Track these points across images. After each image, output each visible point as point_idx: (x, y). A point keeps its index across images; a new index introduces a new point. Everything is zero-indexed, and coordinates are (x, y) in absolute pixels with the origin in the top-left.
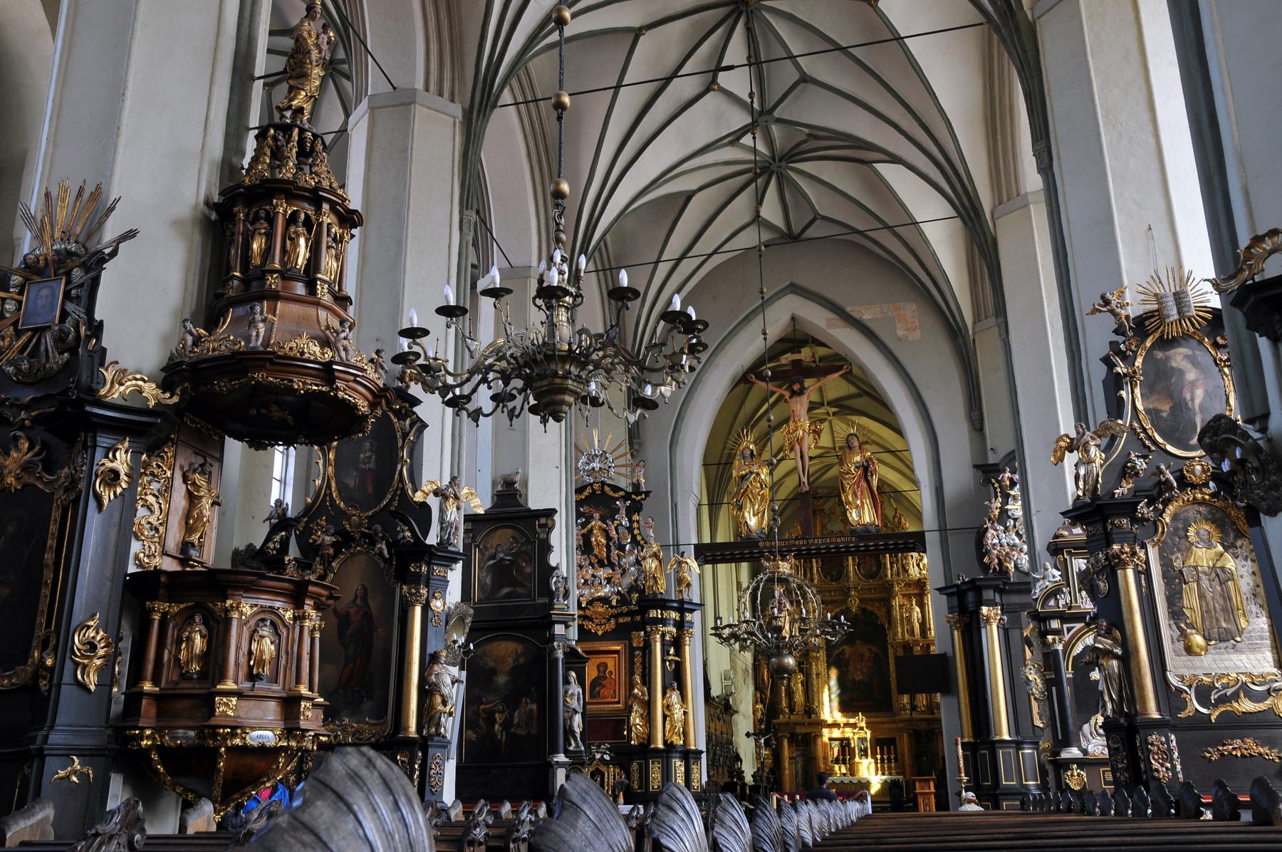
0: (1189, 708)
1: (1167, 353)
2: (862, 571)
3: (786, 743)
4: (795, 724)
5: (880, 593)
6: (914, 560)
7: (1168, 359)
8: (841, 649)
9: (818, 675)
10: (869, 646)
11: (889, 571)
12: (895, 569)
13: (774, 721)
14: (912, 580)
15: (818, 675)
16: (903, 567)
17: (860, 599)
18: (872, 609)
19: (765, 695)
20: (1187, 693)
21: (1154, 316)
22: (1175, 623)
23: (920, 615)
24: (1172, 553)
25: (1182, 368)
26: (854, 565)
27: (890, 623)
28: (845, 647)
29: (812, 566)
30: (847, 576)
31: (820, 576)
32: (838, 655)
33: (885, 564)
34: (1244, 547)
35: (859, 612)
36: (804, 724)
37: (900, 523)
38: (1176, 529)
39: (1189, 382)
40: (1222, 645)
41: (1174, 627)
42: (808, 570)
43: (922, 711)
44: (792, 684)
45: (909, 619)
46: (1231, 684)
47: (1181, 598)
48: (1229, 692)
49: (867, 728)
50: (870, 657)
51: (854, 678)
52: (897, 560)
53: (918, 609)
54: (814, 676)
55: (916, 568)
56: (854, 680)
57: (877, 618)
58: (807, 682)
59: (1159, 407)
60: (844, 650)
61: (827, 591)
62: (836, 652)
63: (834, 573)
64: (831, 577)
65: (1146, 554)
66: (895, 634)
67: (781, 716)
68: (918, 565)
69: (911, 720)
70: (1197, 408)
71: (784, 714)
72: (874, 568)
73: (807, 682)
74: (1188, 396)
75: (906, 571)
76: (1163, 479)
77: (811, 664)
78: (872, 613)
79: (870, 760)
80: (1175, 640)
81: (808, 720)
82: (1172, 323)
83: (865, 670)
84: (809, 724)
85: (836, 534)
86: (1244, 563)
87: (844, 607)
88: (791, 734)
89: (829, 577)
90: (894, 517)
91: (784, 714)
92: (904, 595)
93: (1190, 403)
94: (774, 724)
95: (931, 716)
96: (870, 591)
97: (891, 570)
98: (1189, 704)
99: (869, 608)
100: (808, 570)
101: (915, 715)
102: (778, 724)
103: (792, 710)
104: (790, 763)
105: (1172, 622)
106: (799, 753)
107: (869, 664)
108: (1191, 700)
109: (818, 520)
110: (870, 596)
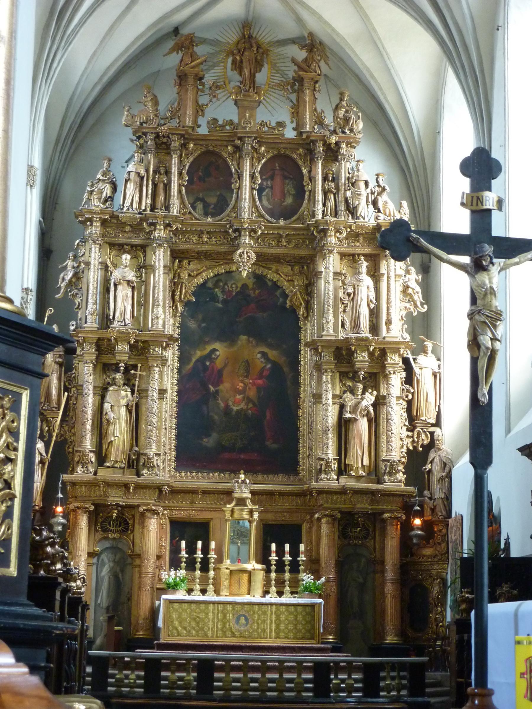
2: (265, 202)
3: (83, 521)
4: (108, 484)
5: (296, 246)
6: (369, 190)
8: (209, 348)
9: (162, 392)
10: (266, 350)
11: (320, 207)
12: (331, 204)
13: (65, 477)
14: (362, 227)
15: (162, 392)
16: (346, 200)
17: (258, 255)
18: (276, 277)
19: (48, 423)
23: (372, 295)
26: (252, 189)
27: (308, 307)
28: (217, 345)
29: (170, 181)
30: (237, 208)
31: (182, 202)
32: (202, 360)
33: (313, 192)
35: (250, 283)
36: (126, 486)
37: (347, 120)
42: (161, 186)
43: (359, 478)
44: (107, 406)
45: (353, 296)
49: (253, 502)
50: (263, 369)
51: (227, 406)
52: (337, 188)
53: (367, 281)
54: (156, 395)
55: (371, 206)
56: (227, 410)
57: (285, 296)
58: (137, 405)
60: (215, 350)
61: (193, 233)
62: (199, 354)
63: (212, 200)
64: (206, 206)
66: (321, 328)
67: (79, 469)
68: (375, 203)
69: (343, 491)
71: (85, 464)
72: (289, 200)
73: (137, 405)
75: (352, 211)
77: (149, 369)
78: (276, 286)
79: (252, 565)
81: (135, 479)
83: (252, 393)
84: (138, 487)
85: (223, 126)
87: (222, 270)
88: (96, 505)
89: (200, 206)
90: (337, 108)
91: (85, 464)
92: (343, 256)
94: (64, 483)
95: (379, 486)
96: (279, 242)
97: (324, 205)
99: (271, 275)
100: (161, 186)
101: (344, 481)
102: (73, 484)
103: (101, 460)
104: (89, 565)
106: (107, 544)
107: (260, 382)
109: (190, 95)
110: (279, 251)
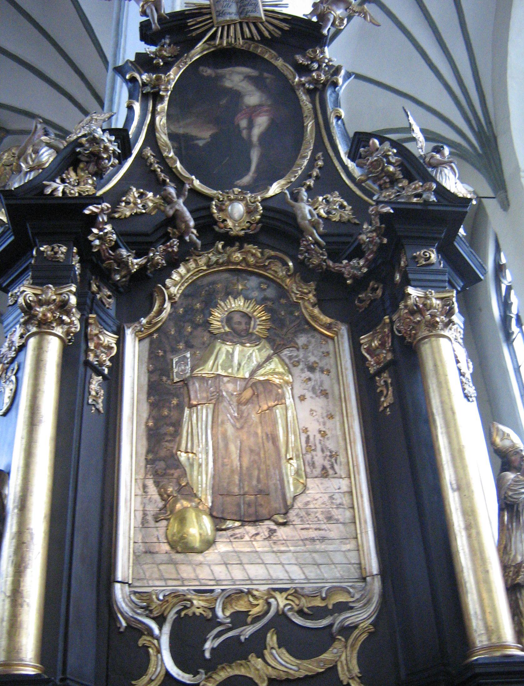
0: (151, 669)
1: (220, 71)
7: (220, 78)
20: (150, 632)
21: (201, 14)
22: (157, 484)
24: (175, 351)
25: (239, 89)
34: (311, 347)
38: (190, 310)
39: (248, 107)
40: (250, 529)
41: (152, 490)
46: (255, 611)
47: (177, 433)
48: (248, 631)
59: (193, 131)
65: (121, 343)
70: (255, 139)
74: (244, 123)
76: (171, 213)
80: (150, 518)
82: (229, 27)
86: (308, 374)
93: (245, 133)
98: (153, 659)
105: (150, 483)
108: (159, 651)
